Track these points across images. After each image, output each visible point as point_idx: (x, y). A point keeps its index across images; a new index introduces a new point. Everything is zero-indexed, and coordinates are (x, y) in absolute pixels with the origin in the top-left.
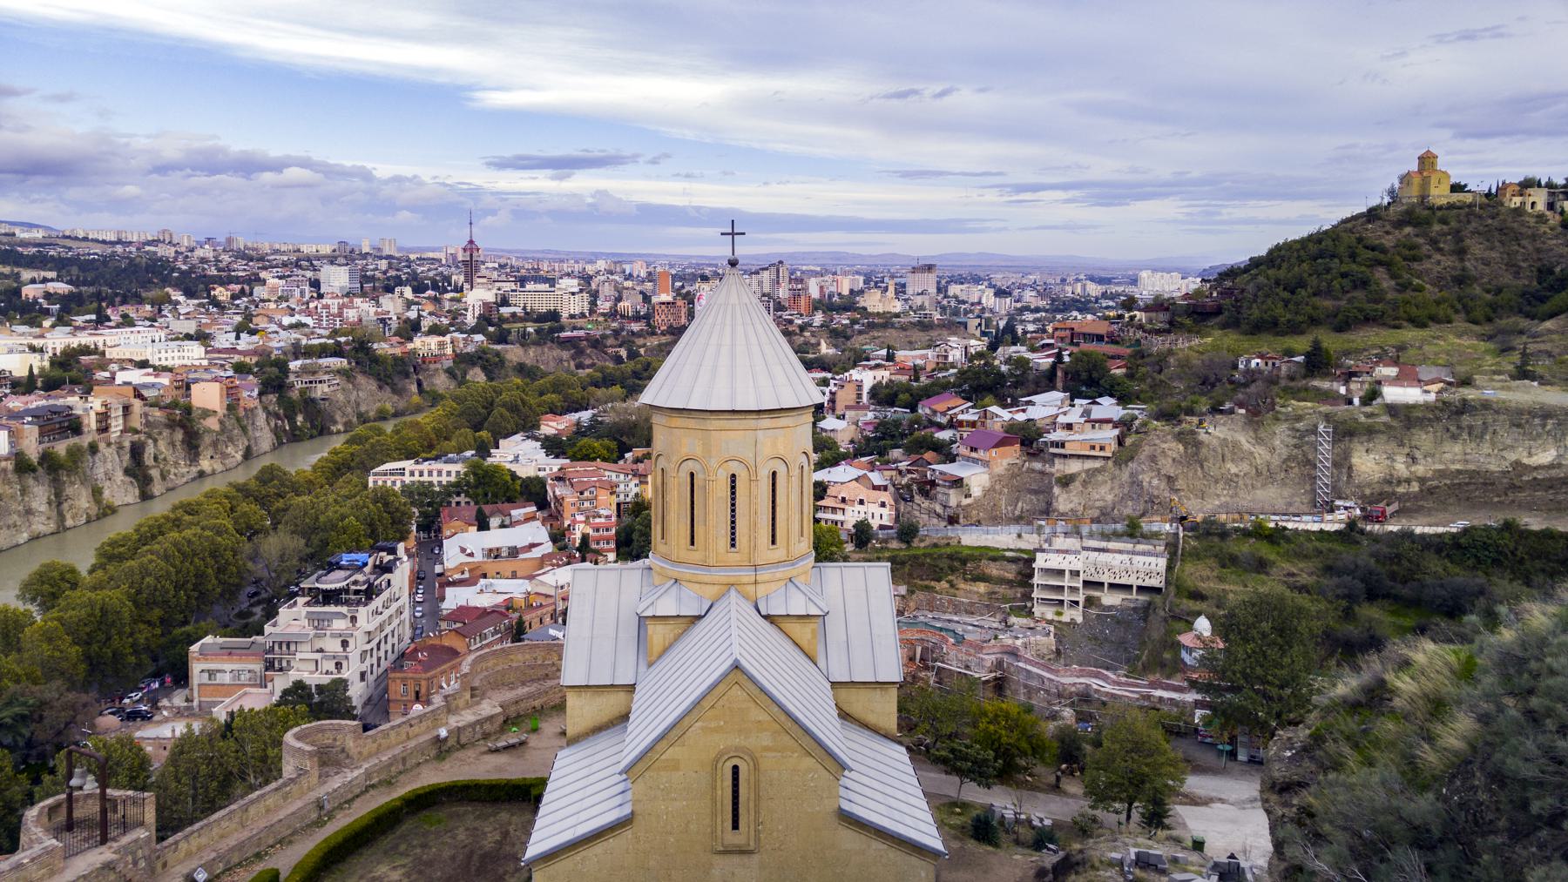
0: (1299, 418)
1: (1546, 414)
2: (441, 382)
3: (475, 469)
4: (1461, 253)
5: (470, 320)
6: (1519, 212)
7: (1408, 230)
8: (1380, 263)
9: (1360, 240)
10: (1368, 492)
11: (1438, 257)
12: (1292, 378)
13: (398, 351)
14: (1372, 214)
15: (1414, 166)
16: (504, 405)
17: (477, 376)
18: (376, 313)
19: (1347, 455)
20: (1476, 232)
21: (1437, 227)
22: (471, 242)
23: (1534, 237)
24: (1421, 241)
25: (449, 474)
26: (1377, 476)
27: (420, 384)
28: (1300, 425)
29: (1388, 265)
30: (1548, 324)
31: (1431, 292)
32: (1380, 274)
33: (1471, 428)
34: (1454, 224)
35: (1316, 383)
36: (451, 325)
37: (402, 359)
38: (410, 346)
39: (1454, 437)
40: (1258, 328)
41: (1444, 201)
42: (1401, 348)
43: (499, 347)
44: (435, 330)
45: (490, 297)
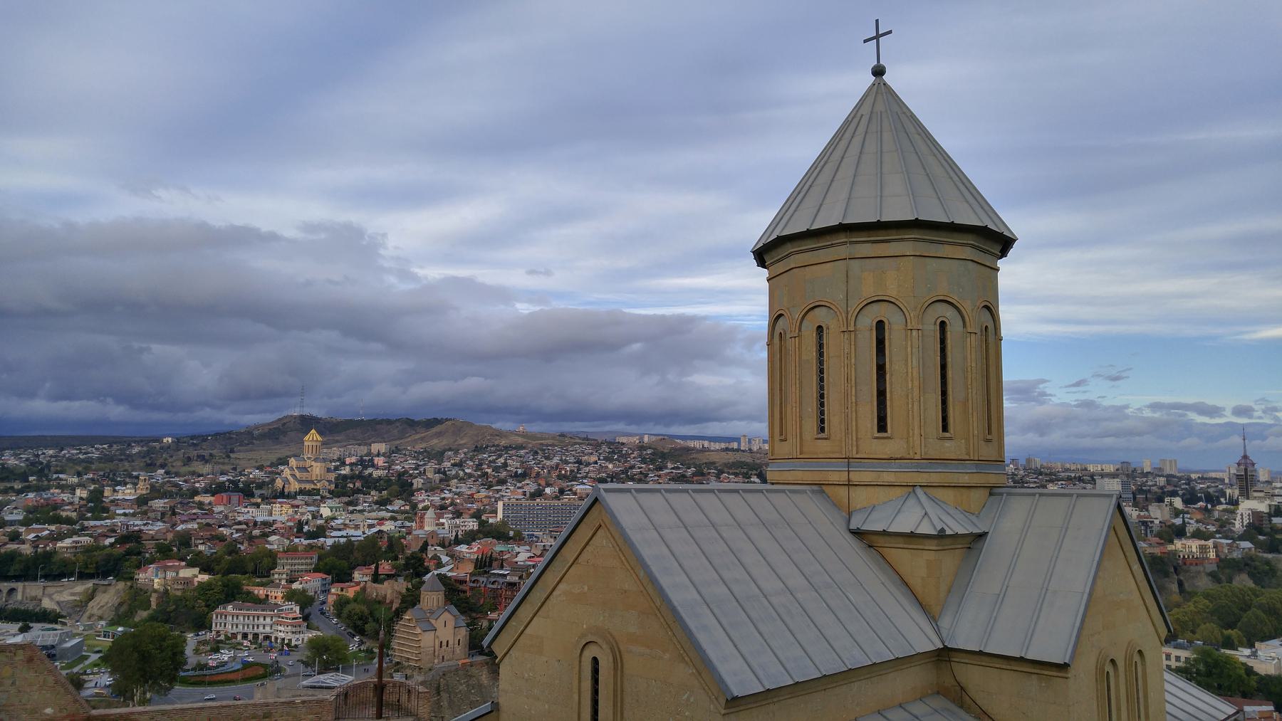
2: (1204, 583)
3: (1204, 655)
5: (1238, 526)
13: (1157, 551)
16: (1260, 607)
17: (1243, 581)
18: (1139, 516)
22: (1245, 457)
25: (1178, 659)
27: (1180, 584)
36: (1217, 532)
37: (1161, 559)
38: (1171, 547)
43: (1270, 556)
44: (1198, 535)
45: (1262, 507)
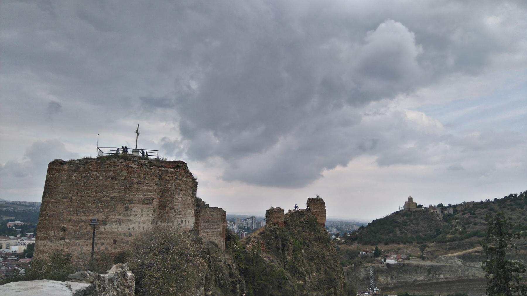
0: (367, 267)
1: (422, 267)
4: (418, 224)
6: (432, 214)
7: (405, 217)
8: (398, 227)
9: (393, 220)
10: (382, 287)
11: (412, 225)
12: (371, 257)
14: (397, 213)
15: (407, 200)
19: (377, 277)
20: (422, 219)
21: (413, 217)
23: (436, 220)
24: (408, 221)
26: (385, 283)
28: (367, 269)
29: (399, 227)
30: (432, 244)
31: (409, 235)
32: (397, 229)
33: (405, 270)
34: (417, 216)
35: (377, 258)
39: (402, 273)
40: (366, 244)
41: (414, 210)
42: (399, 249)
